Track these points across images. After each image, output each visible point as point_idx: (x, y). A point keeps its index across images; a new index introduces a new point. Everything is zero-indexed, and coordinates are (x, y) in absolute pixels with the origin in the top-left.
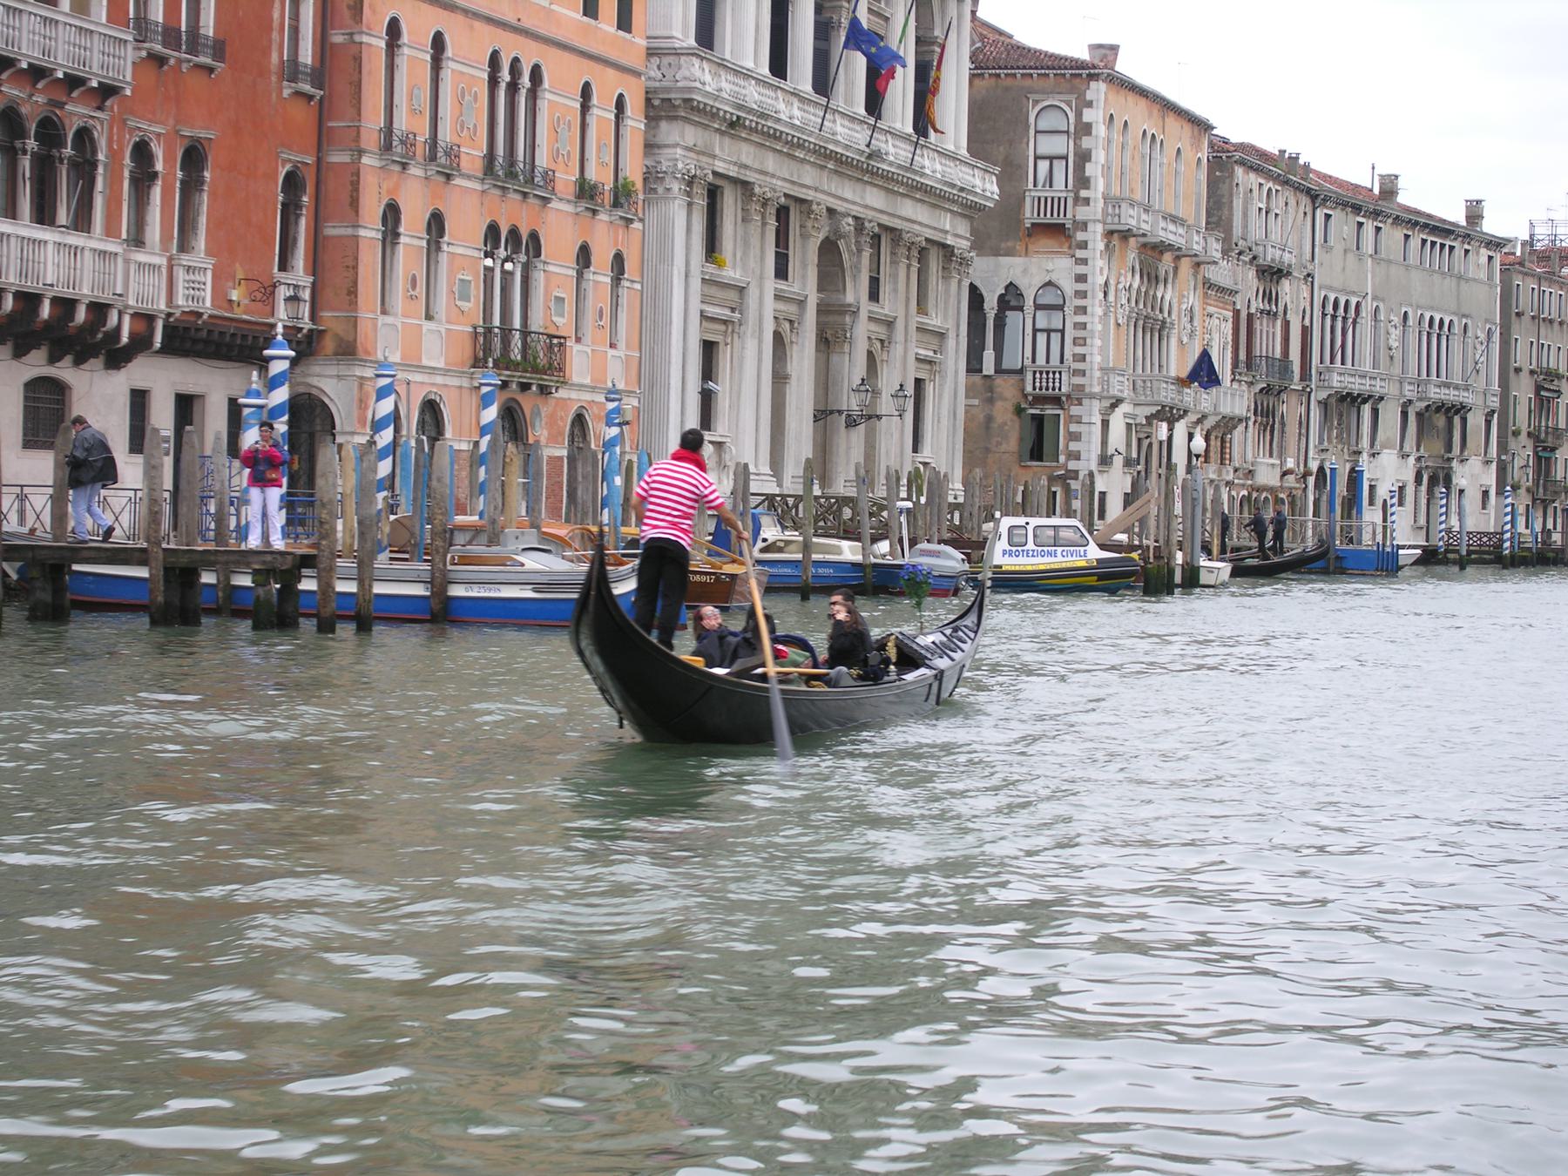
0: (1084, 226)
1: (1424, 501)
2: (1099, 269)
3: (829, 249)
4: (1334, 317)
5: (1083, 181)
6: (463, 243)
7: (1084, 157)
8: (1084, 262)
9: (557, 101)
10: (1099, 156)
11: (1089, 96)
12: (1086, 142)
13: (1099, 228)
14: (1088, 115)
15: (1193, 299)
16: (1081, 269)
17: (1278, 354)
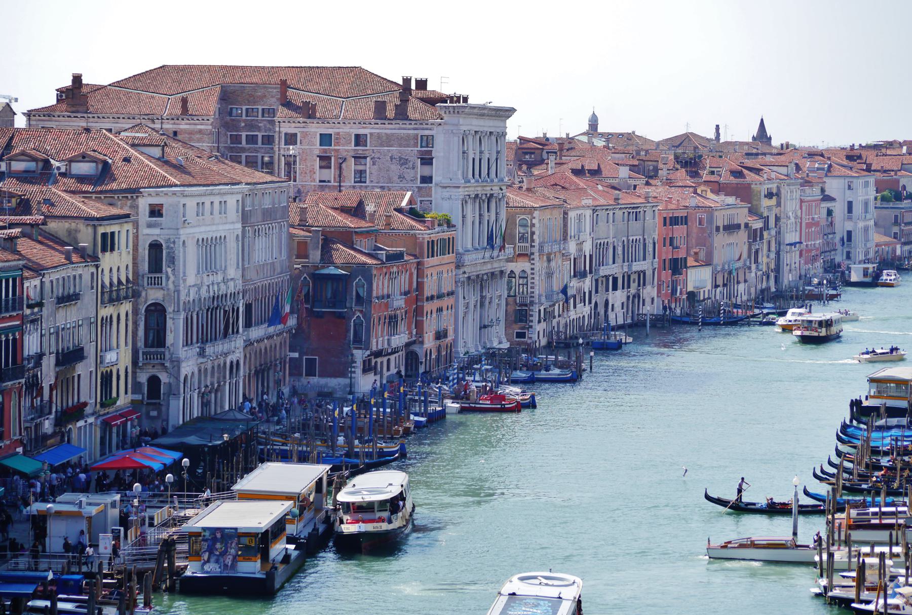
0: (532, 254)
3: (481, 285)
5: (533, 241)
7: (533, 233)
9: (445, 275)
10: (537, 233)
12: (533, 229)
14: (534, 221)
15: (560, 262)
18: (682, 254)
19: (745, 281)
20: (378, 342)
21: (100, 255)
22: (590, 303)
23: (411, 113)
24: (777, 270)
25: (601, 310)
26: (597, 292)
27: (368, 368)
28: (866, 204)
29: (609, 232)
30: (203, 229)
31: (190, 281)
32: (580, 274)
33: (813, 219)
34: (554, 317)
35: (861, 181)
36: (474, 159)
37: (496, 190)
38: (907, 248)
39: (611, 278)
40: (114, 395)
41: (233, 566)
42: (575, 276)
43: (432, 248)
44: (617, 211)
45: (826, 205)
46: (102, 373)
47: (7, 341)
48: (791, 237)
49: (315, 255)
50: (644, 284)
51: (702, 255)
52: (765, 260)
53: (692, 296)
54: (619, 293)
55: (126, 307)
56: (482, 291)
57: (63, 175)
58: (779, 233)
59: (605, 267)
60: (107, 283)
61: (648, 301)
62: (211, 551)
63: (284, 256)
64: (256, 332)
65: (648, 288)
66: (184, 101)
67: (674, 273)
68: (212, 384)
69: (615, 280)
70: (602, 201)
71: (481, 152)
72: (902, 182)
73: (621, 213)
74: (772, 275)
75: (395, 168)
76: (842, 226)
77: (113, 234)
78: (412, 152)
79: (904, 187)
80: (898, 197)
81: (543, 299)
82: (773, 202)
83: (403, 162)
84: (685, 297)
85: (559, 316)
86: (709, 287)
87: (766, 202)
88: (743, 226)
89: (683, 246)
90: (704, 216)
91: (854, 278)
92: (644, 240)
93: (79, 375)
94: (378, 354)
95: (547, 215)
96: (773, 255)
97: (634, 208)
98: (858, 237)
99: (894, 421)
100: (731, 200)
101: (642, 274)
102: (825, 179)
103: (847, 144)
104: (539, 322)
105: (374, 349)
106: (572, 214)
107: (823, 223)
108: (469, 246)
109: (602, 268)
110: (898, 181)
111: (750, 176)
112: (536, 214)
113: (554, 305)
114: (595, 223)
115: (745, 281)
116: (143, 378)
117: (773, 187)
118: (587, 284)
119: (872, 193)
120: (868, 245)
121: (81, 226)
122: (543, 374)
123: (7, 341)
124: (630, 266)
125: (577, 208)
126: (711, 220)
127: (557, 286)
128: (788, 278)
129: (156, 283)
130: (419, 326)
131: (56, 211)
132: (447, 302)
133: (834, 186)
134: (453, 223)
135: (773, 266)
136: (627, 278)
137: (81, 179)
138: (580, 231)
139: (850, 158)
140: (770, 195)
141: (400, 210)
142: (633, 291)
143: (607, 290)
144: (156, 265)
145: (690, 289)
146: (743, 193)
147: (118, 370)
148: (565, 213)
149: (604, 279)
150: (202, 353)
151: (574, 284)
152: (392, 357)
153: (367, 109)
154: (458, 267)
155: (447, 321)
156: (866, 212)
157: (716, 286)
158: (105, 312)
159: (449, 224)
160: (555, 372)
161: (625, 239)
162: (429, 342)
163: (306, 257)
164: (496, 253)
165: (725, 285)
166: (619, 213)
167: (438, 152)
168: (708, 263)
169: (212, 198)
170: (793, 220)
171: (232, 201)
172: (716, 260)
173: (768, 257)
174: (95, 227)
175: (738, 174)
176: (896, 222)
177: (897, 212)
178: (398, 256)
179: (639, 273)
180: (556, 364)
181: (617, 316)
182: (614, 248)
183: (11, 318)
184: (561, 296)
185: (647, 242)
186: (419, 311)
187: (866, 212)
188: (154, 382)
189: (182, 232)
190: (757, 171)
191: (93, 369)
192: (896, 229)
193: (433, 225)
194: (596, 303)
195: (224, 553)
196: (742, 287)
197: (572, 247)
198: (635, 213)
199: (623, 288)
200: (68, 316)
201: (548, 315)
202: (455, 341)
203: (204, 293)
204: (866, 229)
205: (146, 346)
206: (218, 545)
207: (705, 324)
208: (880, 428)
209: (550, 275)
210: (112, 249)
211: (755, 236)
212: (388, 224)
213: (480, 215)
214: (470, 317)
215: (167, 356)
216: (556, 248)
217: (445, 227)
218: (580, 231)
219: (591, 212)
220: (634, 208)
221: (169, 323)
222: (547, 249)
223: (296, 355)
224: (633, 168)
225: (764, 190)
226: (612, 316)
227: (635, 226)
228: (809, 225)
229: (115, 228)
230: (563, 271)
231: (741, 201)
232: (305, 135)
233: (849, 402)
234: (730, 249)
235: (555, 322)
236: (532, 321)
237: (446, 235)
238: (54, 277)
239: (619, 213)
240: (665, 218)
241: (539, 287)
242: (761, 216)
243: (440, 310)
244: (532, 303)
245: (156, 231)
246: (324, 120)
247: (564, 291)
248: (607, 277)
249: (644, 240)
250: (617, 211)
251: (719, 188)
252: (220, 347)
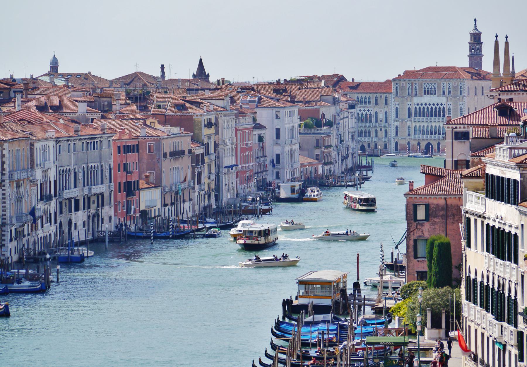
1: (91, 224)
4: (63, 175)
8: (4, 190)
10: (7, 162)
11: (4, 147)
12: (4, 159)
13: (8, 181)
14: (4, 152)
15: (28, 187)
16: (4, 192)
17: (48, 193)
18: (134, 178)
19: (190, 200)
22: (55, 222)
24: (218, 189)
25: (65, 229)
26: (61, 213)
28: (292, 130)
29: (69, 160)
32: (46, 198)
33: (247, 144)
34: (24, 236)
35: (287, 111)
38: (327, 167)
39: (73, 201)
42: (41, 199)
44: (77, 142)
45: (257, 132)
48: (229, 161)
50: (103, 205)
51: (152, 179)
52: (207, 181)
53: (144, 214)
54: (80, 213)
58: (218, 157)
59: (68, 191)
61: (106, 219)
65: (106, 208)
67: (128, 195)
69: (77, 202)
70: (64, 133)
72: (322, 111)
73: (80, 143)
74: (213, 194)
76: (272, 149)
79: (323, 115)
80: (319, 124)
81: (14, 220)
82: (212, 130)
84: (138, 215)
85: (29, 235)
86: (159, 206)
87: (206, 131)
88: (186, 152)
89: (136, 171)
90: (153, 144)
91: (283, 194)
92: (102, 166)
95: (16, 146)
96: (213, 177)
97: (91, 139)
98: (285, 160)
99: (320, 317)
100: (176, 130)
101: (100, 196)
102: (256, 110)
103: (274, 80)
104: (11, 240)
106: (38, 146)
107: (256, 148)
109: (65, 191)
110: (318, 111)
111: (192, 109)
112: (6, 146)
113: (23, 225)
114: (58, 152)
115: (190, 200)
117: (212, 118)
118: (53, 206)
119: (296, 121)
120: (294, 166)
122: (16, 286)
124: (90, 190)
125: (42, 140)
126: (159, 148)
127: (25, 209)
128: (227, 196)
133: (264, 116)
135: (213, 186)
136: (88, 200)
138: (44, 160)
139: (277, 91)
140: (209, 125)
142: (93, 211)
143: (70, 211)
145: (143, 208)
146: (186, 123)
148: (32, 145)
149: (67, 201)
151: (41, 206)
156: (292, 137)
157: (165, 205)
160: (27, 284)
161: (85, 166)
165: (172, 204)
166: (79, 144)
168: (157, 185)
170: (229, 146)
172: (164, 182)
173: (209, 178)
175: (181, 107)
176: (318, 146)
177: (318, 137)
179: (98, 195)
180: (27, 277)
181: (80, 234)
182: (75, 173)
184: (30, 217)
185: (104, 168)
187: (292, 137)
190: (198, 104)
192: (317, 152)
194: (61, 223)
196: (187, 205)
197: (38, 174)
198: (93, 143)
199: (84, 209)
201: (19, 235)
204: (292, 152)
207: (155, 238)
208: (308, 324)
209: (19, 199)
211: (197, 160)
216: (24, 175)
218: (44, 160)
219: (54, 143)
220: (91, 139)
222: (16, 177)
224: (90, 104)
225: (204, 120)
226: (75, 234)
227: (93, 154)
228: (243, 150)
230: (31, 195)
231: (185, 131)
233: (281, 302)
234: (175, 172)
235: (24, 240)
236: (4, 240)
239: (79, 144)
240: (119, 147)
242: (202, 144)
247: (32, 213)
248: (70, 200)
249: (102, 166)
250: (77, 142)
251: (165, 120)
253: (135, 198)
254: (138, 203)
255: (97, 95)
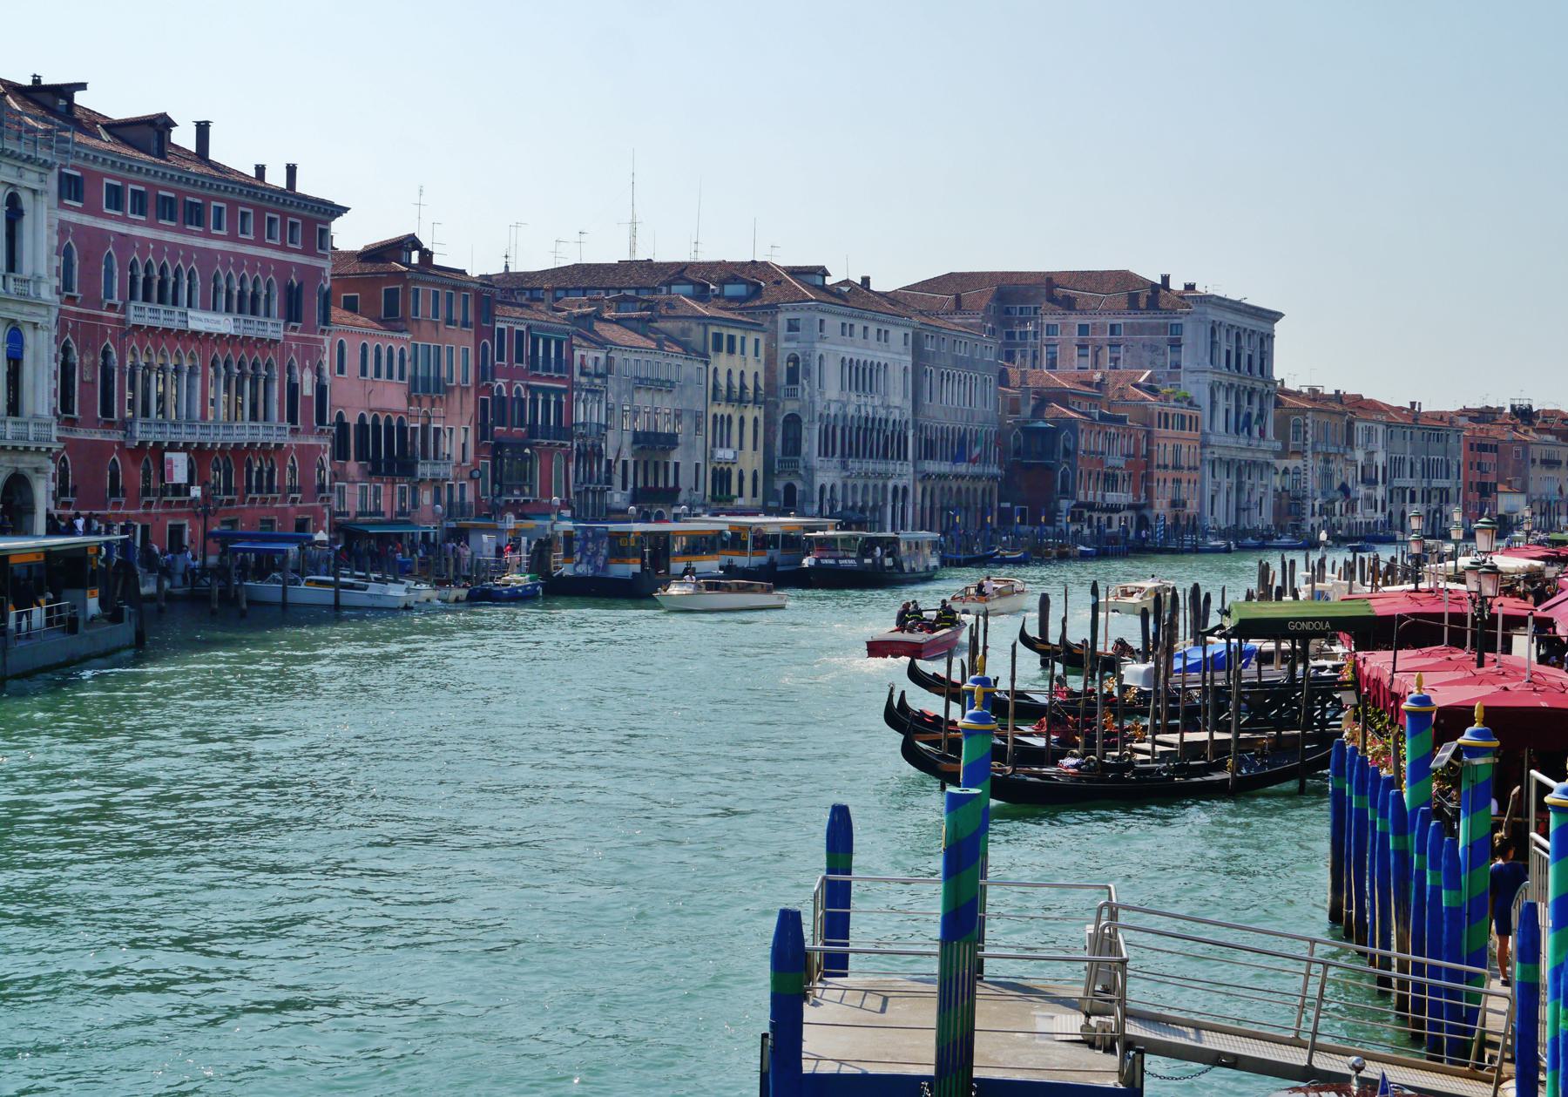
2: (1310, 463)
6: (1169, 484)
9: (1185, 450)
15: (1342, 465)
18: (1491, 479)
20: (1088, 493)
21: (711, 353)
22: (1383, 510)
23: (1163, 303)
27: (1076, 517)
29: (1406, 450)
30: (850, 349)
31: (830, 394)
32: (1370, 482)
36: (1228, 352)
37: (1259, 385)
40: (734, 491)
41: (605, 567)
43: (1165, 420)
46: (714, 469)
47: (547, 403)
49: (1027, 411)
51: (1518, 484)
54: (1417, 505)
55: (752, 413)
56: (1239, 475)
57: (717, 296)
60: (723, 380)
62: (583, 550)
63: (990, 408)
64: (932, 466)
66: (958, 299)
68: (865, 503)
69: (1413, 494)
71: (1238, 348)
75: (1146, 354)
77: (731, 339)
78: (1163, 339)
81: (1318, 493)
83: (1154, 349)
93: (677, 465)
94: (1091, 507)
95: (1324, 419)
100: (1550, 438)
104: (1313, 514)
105: (1082, 498)
106: (1359, 425)
108: (1222, 429)
112: (1309, 414)
113: (1332, 502)
116: (780, 485)
121: (693, 326)
123: (547, 403)
125: (1366, 420)
127: (1336, 485)
129: (792, 395)
130: (1149, 492)
131: (671, 313)
132: (1185, 475)
134: (1196, 401)
137: (732, 299)
141: (1137, 386)
142: (1433, 506)
143: (1404, 501)
144: (793, 377)
145: (1501, 511)
147: (741, 472)
148: (1350, 424)
150: (844, 467)
151: (1362, 491)
152: (1115, 517)
153: (1122, 299)
154: (1204, 445)
155: (1185, 491)
158: (723, 410)
159: (1191, 403)
162: (1161, 507)
163: (1018, 412)
164: (1255, 442)
166: (1418, 433)
167: (1187, 338)
168: (1523, 490)
169: (865, 323)
171: (897, 334)
172: (1532, 488)
174: (705, 326)
178: (1122, 420)
179: (1441, 490)
183: (550, 378)
186: (1148, 477)
188: (790, 489)
189: (817, 345)
191: (701, 462)
193: (1167, 399)
194: (1391, 514)
195: (595, 554)
197: (1360, 456)
200: (666, 403)
201: (1326, 511)
202: (1200, 515)
203: (851, 410)
205: (784, 453)
206: (590, 545)
209: (1327, 476)
210: (731, 351)
212: (1121, 396)
213: (1238, 407)
214: (1222, 498)
215: (801, 464)
217: (1185, 404)
221: (805, 433)
223: (1008, 505)
229: (738, 334)
232: (1064, 325)
235: (1334, 520)
237: (1188, 412)
238: (632, 357)
239: (1418, 433)
241: (1312, 482)
243: (1178, 481)
244: (1305, 497)
245: (794, 345)
246: (1083, 312)
247: (1344, 489)
248: (1404, 490)
252: (870, 465)
253: (1491, 500)
254: (1496, 506)
255: (1485, 415)
